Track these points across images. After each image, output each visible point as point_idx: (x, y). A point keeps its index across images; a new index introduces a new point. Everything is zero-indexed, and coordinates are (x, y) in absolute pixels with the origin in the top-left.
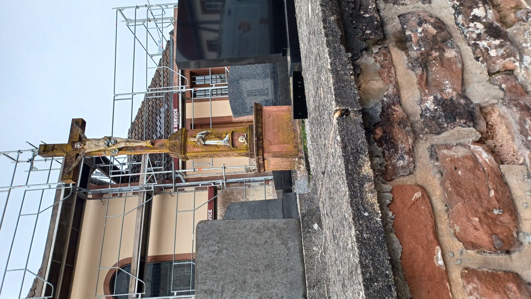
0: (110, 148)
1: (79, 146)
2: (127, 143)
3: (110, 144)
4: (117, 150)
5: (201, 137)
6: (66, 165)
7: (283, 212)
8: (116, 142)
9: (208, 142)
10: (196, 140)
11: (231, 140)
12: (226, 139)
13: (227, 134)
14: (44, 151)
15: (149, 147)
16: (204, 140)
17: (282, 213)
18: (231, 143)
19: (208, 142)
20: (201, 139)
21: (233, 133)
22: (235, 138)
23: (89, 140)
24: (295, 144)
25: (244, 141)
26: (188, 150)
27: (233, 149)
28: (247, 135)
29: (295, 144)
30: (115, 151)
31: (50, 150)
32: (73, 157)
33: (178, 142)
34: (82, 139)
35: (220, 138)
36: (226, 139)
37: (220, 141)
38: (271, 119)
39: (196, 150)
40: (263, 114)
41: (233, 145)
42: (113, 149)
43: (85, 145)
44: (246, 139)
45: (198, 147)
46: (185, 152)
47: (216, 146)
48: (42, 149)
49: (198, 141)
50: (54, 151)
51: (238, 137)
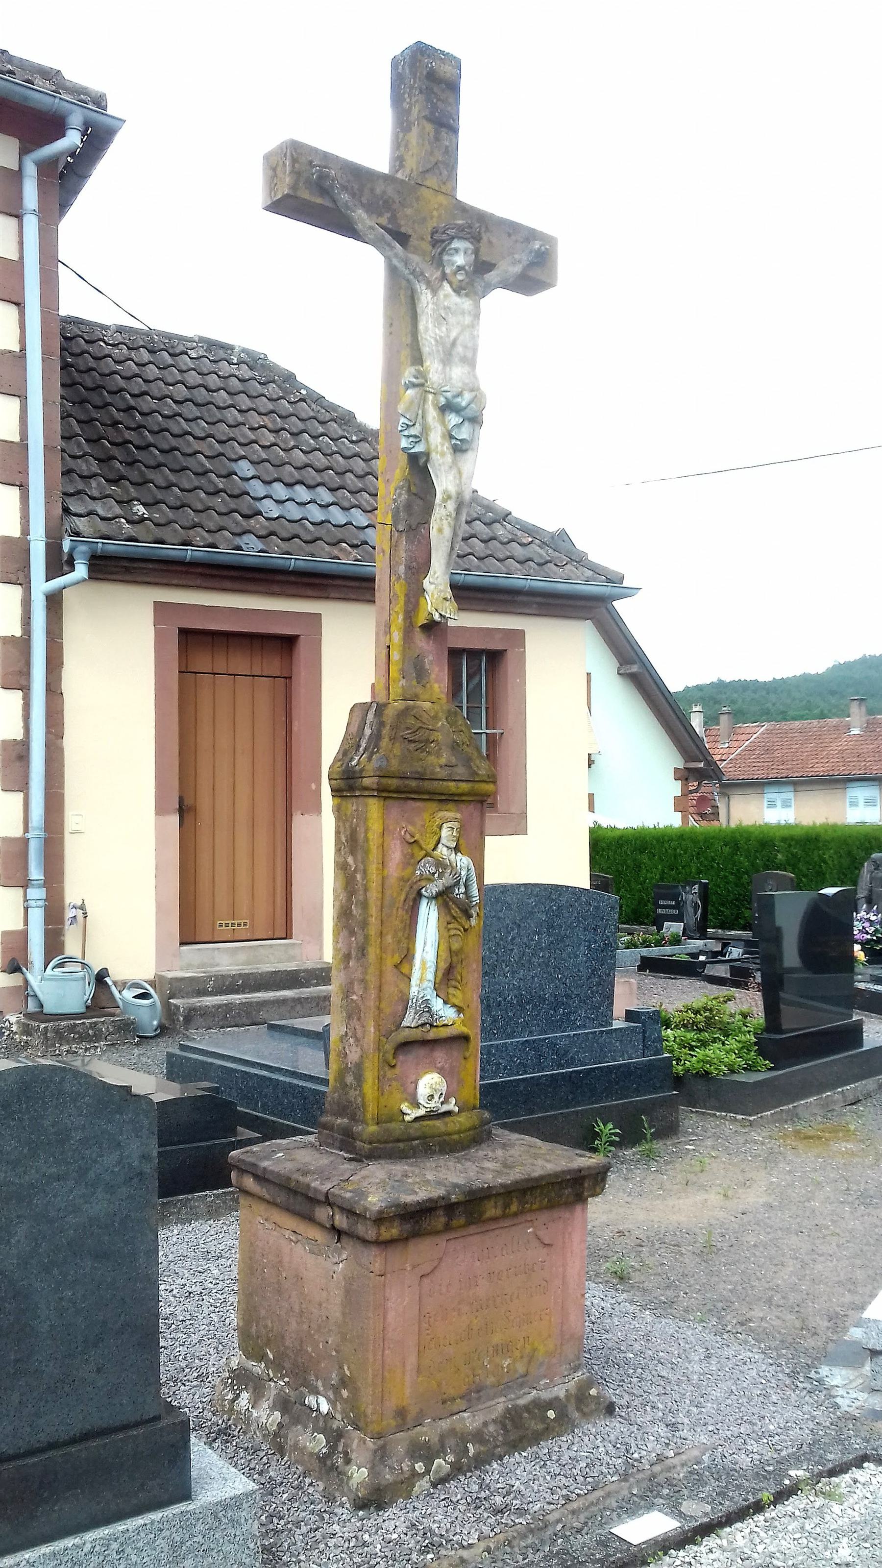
0: (432, 414)
1: (460, 260)
2: (451, 506)
3: (453, 419)
4: (419, 448)
5: (457, 884)
6: (359, 176)
7: (86, 1436)
8: (459, 448)
9: (429, 918)
10: (442, 851)
11: (432, 1034)
12: (437, 1005)
13: (460, 1010)
14: (432, 76)
15: (417, 605)
16: (444, 897)
17: (77, 1427)
18: (417, 1034)
19: (429, 918)
20: (447, 880)
21: (464, 1039)
22: (440, 1055)
23: (477, 306)
24: (413, 1411)
25: (426, 1105)
26: (395, 809)
27: (389, 1047)
28: (448, 1113)
29: (413, 1411)
30: (417, 439)
31: (434, 107)
32: (393, 219)
33: (438, 761)
34: (478, 277)
35: (447, 978)
36: (437, 1005)
37: (430, 976)
38: (537, 1254)
39: (396, 855)
40: (556, 1213)
41: (405, 1046)
42: (426, 429)
43: (458, 290)
44: (431, 1115)
45: (410, 861)
46: (383, 793)
47: (408, 956)
48: (446, 70)
49: (441, 864)
50: (429, 127)
51: (441, 1071)
